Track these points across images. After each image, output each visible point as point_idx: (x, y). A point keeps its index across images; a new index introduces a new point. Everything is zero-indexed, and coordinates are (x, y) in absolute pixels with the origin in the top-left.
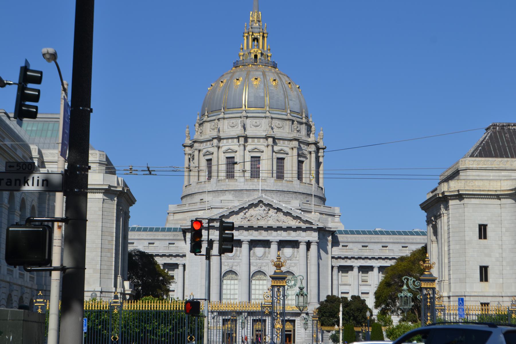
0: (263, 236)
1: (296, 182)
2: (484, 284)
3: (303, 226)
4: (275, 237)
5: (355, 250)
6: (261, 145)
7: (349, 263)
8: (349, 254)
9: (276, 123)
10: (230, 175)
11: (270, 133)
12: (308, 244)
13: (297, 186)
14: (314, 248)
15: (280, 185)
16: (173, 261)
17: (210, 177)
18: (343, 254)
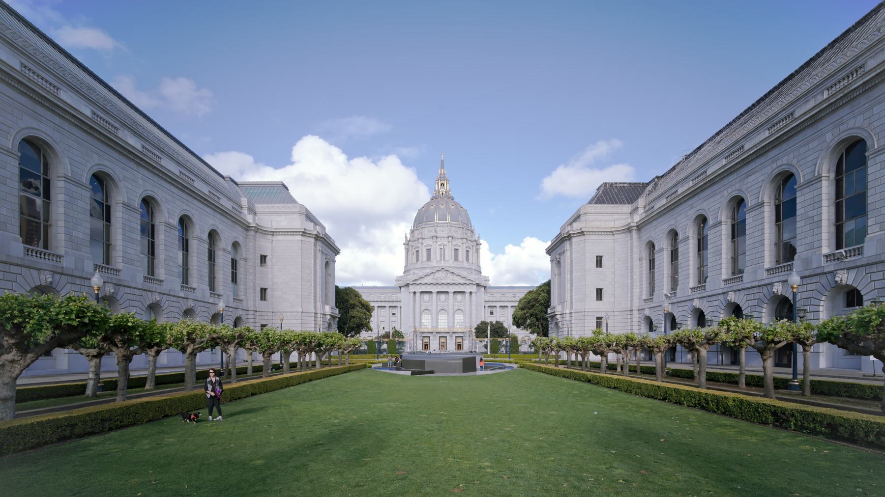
0: (445, 289)
1: (465, 262)
2: (600, 302)
3: (468, 282)
4: (451, 289)
5: (498, 297)
6: (445, 242)
7: (494, 304)
8: (494, 299)
9: (453, 229)
10: (429, 258)
11: (450, 234)
12: (471, 293)
13: (465, 264)
14: (473, 295)
15: (456, 264)
16: (395, 304)
17: (417, 260)
18: (491, 299)
